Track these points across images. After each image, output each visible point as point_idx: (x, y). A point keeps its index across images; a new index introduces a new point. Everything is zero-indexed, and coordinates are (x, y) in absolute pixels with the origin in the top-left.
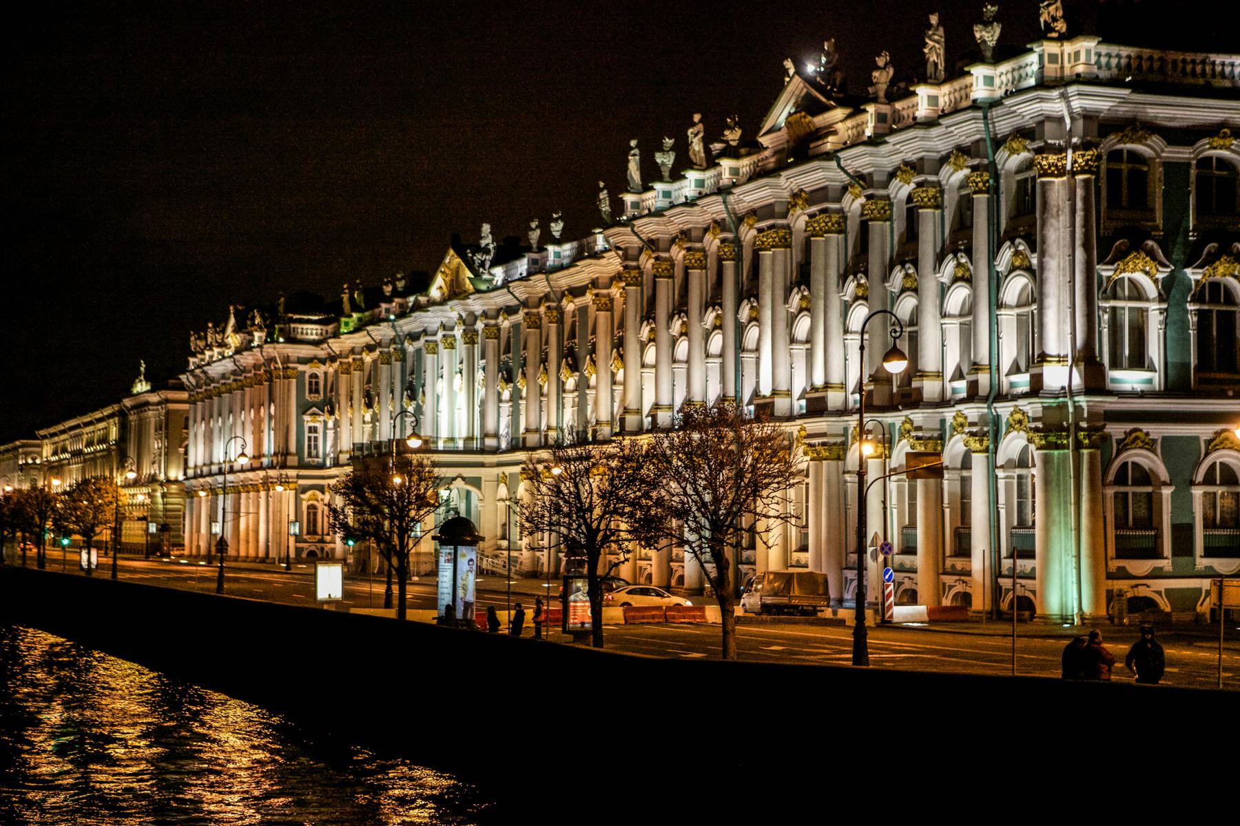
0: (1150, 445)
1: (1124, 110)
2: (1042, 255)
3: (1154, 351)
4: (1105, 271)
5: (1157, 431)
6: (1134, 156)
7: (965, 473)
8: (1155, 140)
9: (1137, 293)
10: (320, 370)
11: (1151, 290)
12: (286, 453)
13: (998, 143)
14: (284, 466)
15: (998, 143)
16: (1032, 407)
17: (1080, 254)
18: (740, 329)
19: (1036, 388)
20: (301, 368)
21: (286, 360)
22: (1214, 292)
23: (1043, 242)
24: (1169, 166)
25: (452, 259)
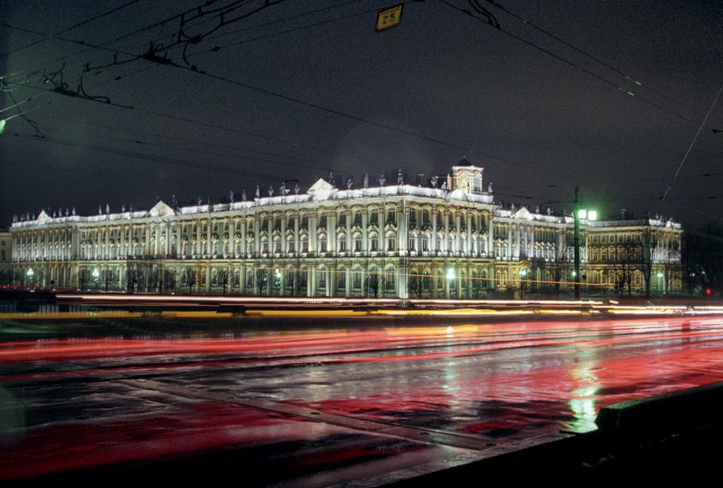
0: (416, 266)
1: (413, 200)
2: (399, 228)
3: (416, 247)
4: (410, 232)
5: (417, 264)
6: (413, 209)
7: (359, 272)
8: (417, 206)
9: (413, 237)
10: (85, 231)
11: (416, 236)
12: (76, 256)
13: (386, 204)
14: (75, 260)
15: (386, 204)
16: (398, 259)
17: (406, 228)
18: (300, 236)
19: (397, 255)
20: (80, 230)
21: (76, 227)
22: (425, 237)
23: (400, 225)
24: (419, 211)
25: (161, 204)
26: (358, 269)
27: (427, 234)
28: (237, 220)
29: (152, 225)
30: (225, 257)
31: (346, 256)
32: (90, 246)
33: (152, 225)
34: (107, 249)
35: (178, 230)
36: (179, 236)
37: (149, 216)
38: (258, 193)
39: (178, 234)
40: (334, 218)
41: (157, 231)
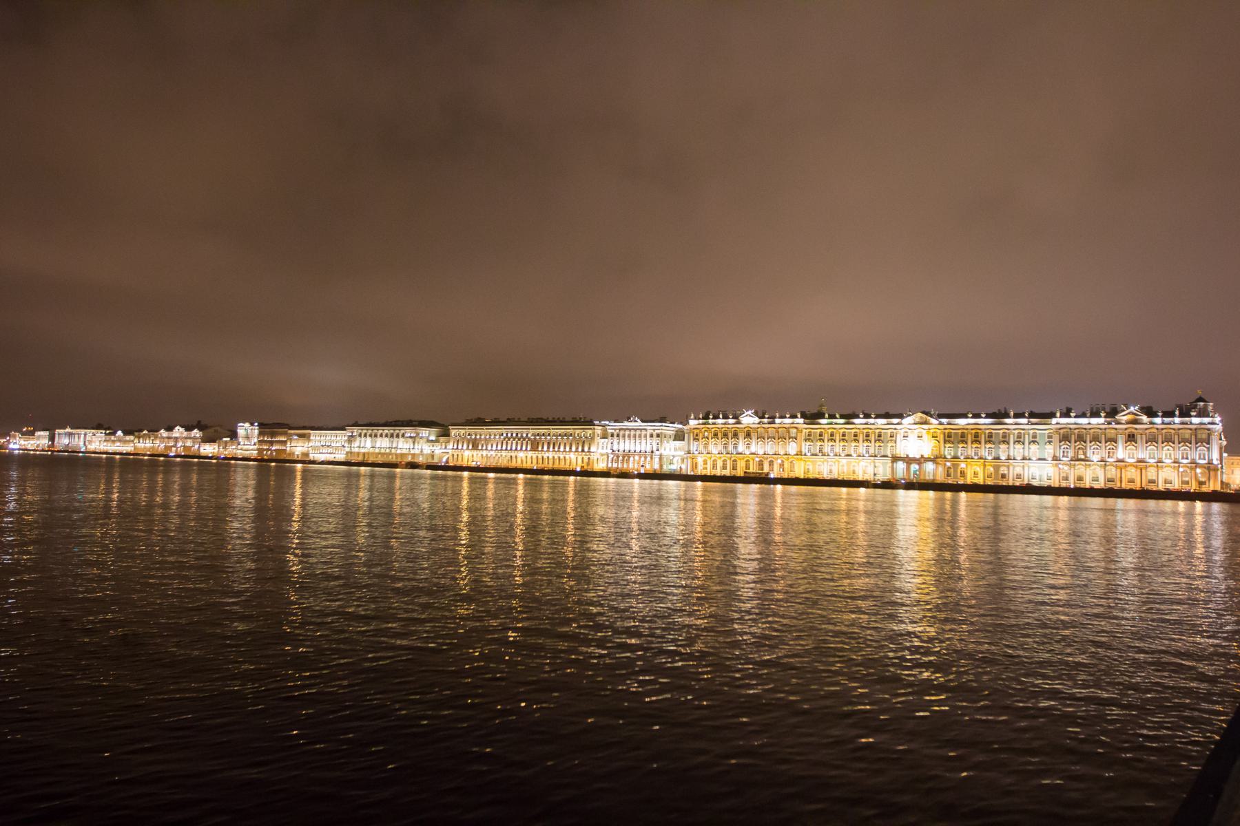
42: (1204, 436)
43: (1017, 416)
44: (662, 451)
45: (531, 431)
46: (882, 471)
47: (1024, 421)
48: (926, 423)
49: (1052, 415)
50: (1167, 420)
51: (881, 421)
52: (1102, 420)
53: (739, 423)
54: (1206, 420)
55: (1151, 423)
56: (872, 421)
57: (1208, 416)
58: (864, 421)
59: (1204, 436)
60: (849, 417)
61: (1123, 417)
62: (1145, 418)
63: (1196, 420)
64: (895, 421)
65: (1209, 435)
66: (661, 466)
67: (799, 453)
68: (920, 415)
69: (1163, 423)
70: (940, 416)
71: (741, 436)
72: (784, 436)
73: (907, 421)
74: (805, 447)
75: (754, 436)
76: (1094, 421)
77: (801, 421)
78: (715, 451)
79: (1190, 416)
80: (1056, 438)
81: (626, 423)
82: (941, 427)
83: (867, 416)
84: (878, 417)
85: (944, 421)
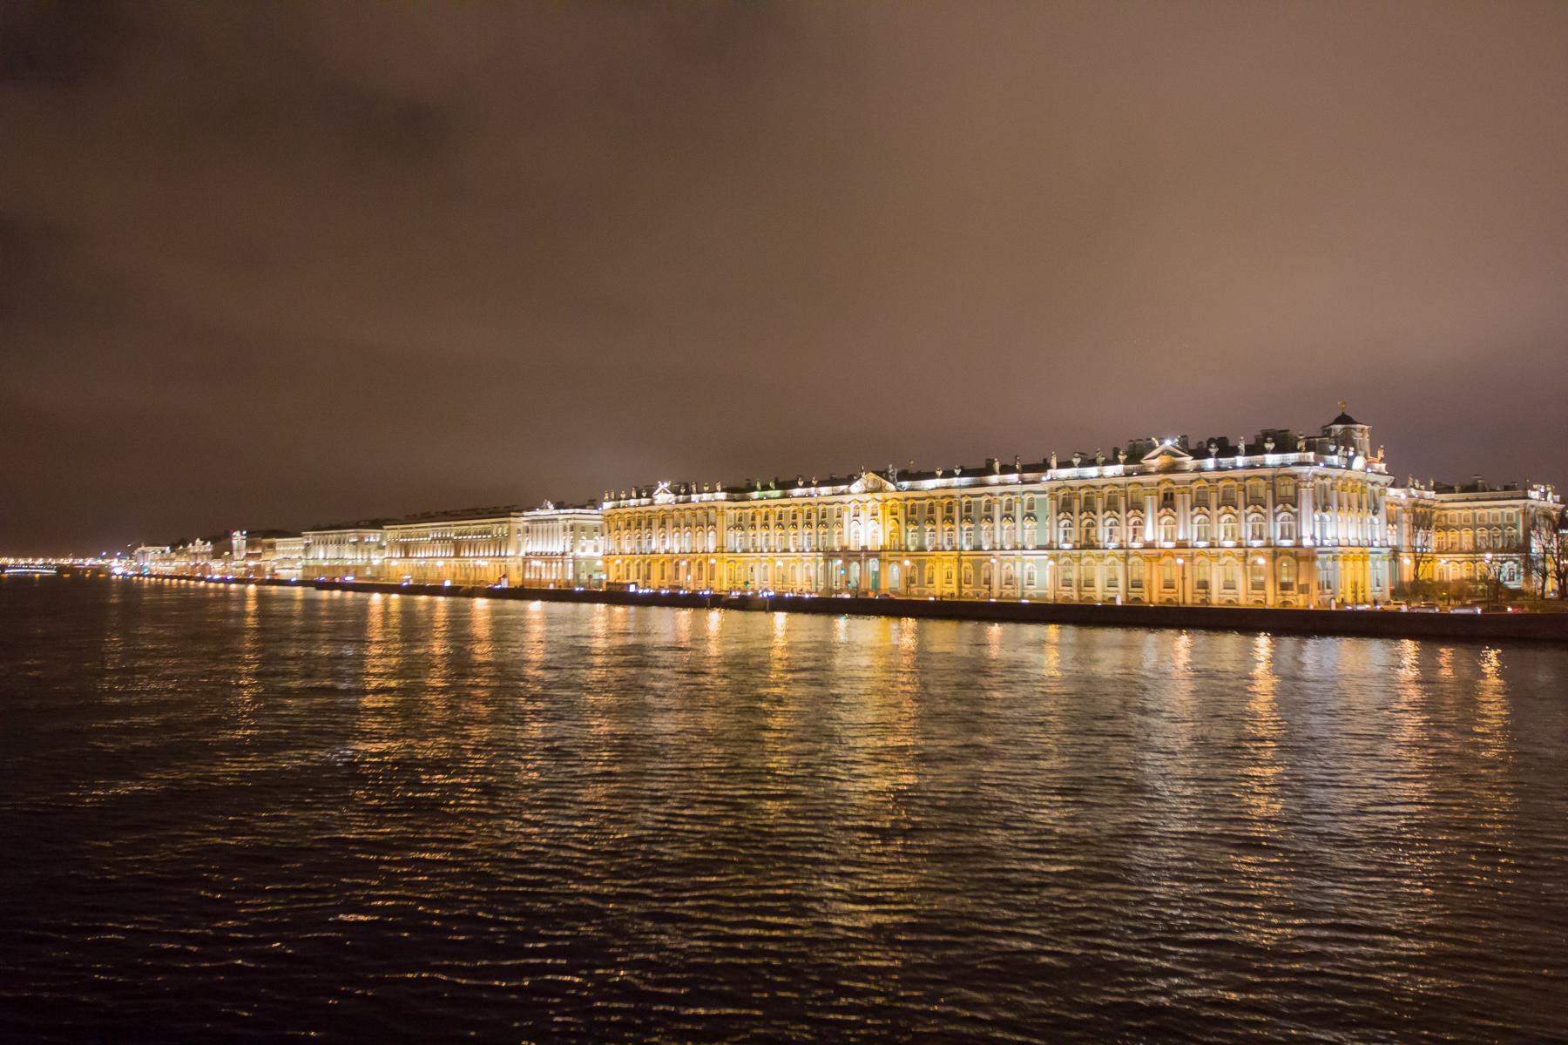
26: (1114, 563)
27: (1327, 516)
28: (806, 508)
29: (852, 506)
30: (986, 547)
31: (1212, 546)
32: (739, 533)
33: (852, 506)
34: (814, 537)
35: (901, 512)
36: (903, 521)
37: (849, 493)
38: (1054, 462)
39: (901, 516)
40: (1188, 496)
41: (862, 514)
42: (1290, 491)
43: (1006, 469)
44: (578, 552)
45: (452, 529)
46: (804, 577)
47: (1014, 477)
48: (880, 489)
49: (1044, 467)
50: (1225, 461)
51: (825, 490)
52: (1119, 469)
53: (652, 504)
54: (1292, 457)
55: (1199, 469)
56: (812, 490)
57: (1294, 450)
58: (804, 491)
59: (1282, 491)
60: (785, 485)
61: (1154, 461)
62: (1189, 462)
63: (1272, 459)
64: (843, 488)
65: (1297, 487)
66: (577, 576)
67: (721, 549)
68: (872, 476)
69: (1218, 469)
70: (904, 476)
71: (656, 523)
72: (704, 521)
73: (857, 487)
74: (733, 539)
75: (669, 522)
76: (1110, 470)
77: (722, 496)
78: (628, 550)
79: (1264, 451)
80: (1050, 505)
81: (538, 512)
82: (901, 495)
83: (807, 484)
84: (821, 484)
85: (906, 484)
